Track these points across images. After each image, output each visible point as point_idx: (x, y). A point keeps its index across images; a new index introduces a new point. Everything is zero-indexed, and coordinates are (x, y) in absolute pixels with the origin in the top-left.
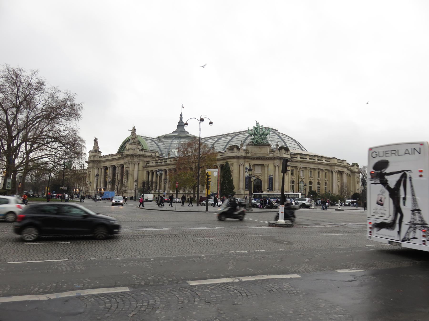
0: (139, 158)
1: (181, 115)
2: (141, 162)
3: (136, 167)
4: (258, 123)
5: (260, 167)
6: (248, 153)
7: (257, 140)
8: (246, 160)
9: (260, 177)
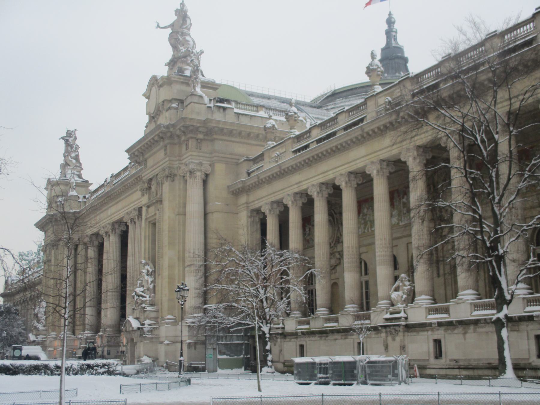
0: (206, 147)
1: (390, 22)
2: (220, 168)
3: (194, 192)
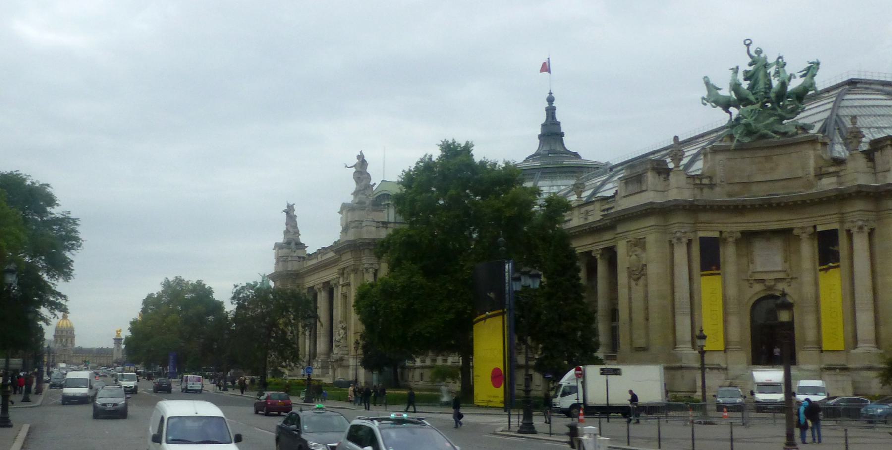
1: (550, 100)
4: (759, 52)
5: (777, 245)
6: (711, 186)
7: (747, 125)
8: (703, 217)
9: (780, 286)
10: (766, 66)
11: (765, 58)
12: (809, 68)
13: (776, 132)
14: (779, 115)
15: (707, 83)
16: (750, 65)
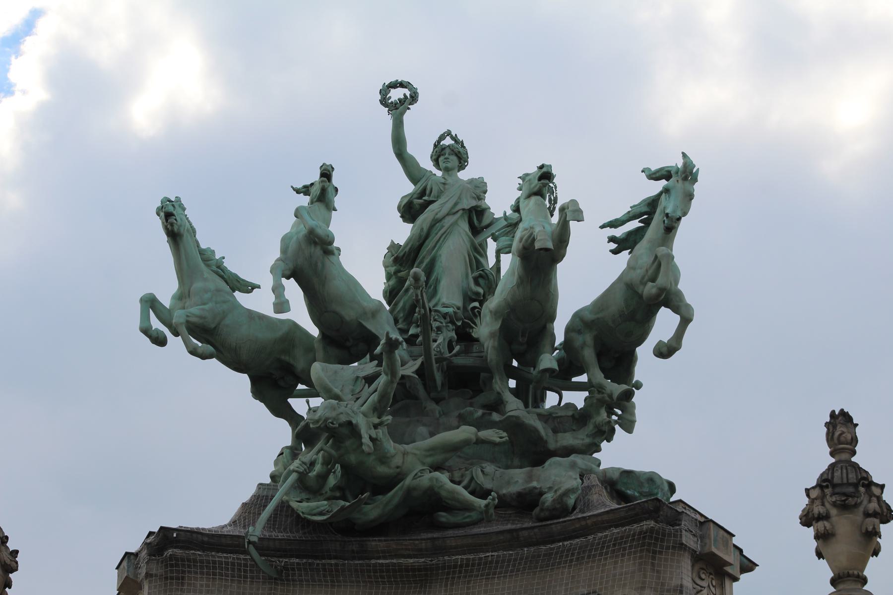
4: (450, 153)
10: (477, 218)
11: (479, 188)
12: (653, 203)
13: (483, 494)
14: (515, 427)
15: (174, 224)
16: (410, 211)
